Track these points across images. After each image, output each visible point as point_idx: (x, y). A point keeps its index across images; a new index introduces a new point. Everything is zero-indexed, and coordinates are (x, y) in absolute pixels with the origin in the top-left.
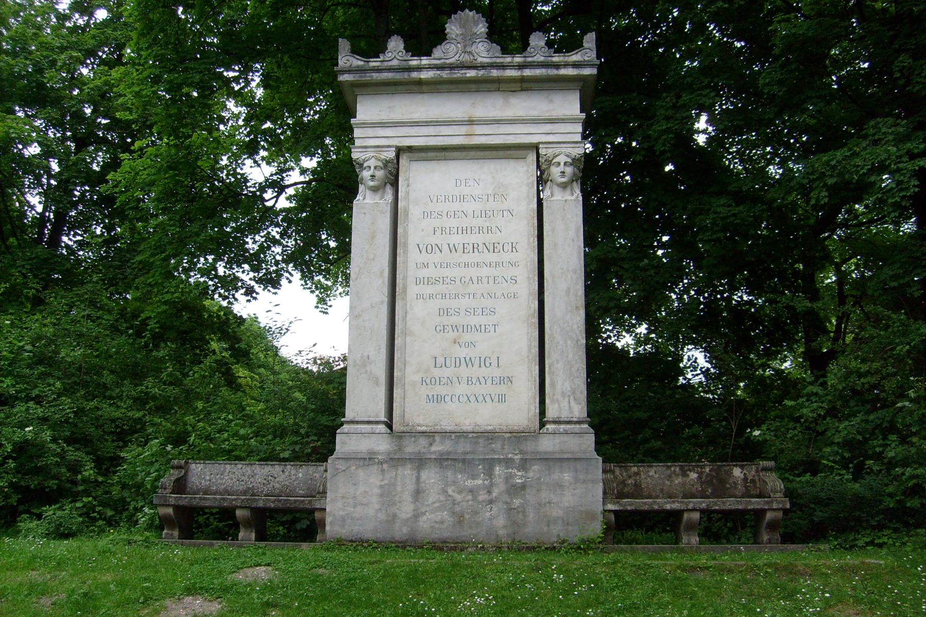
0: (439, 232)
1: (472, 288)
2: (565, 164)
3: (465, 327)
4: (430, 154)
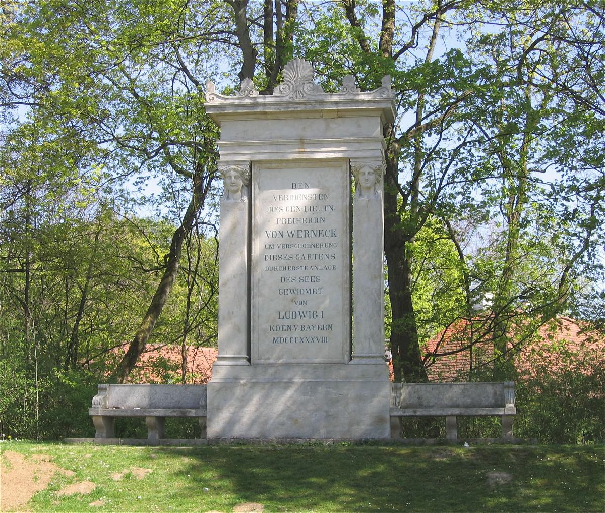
1: (304, 263)
2: (369, 173)
3: (300, 290)
4: (274, 165)
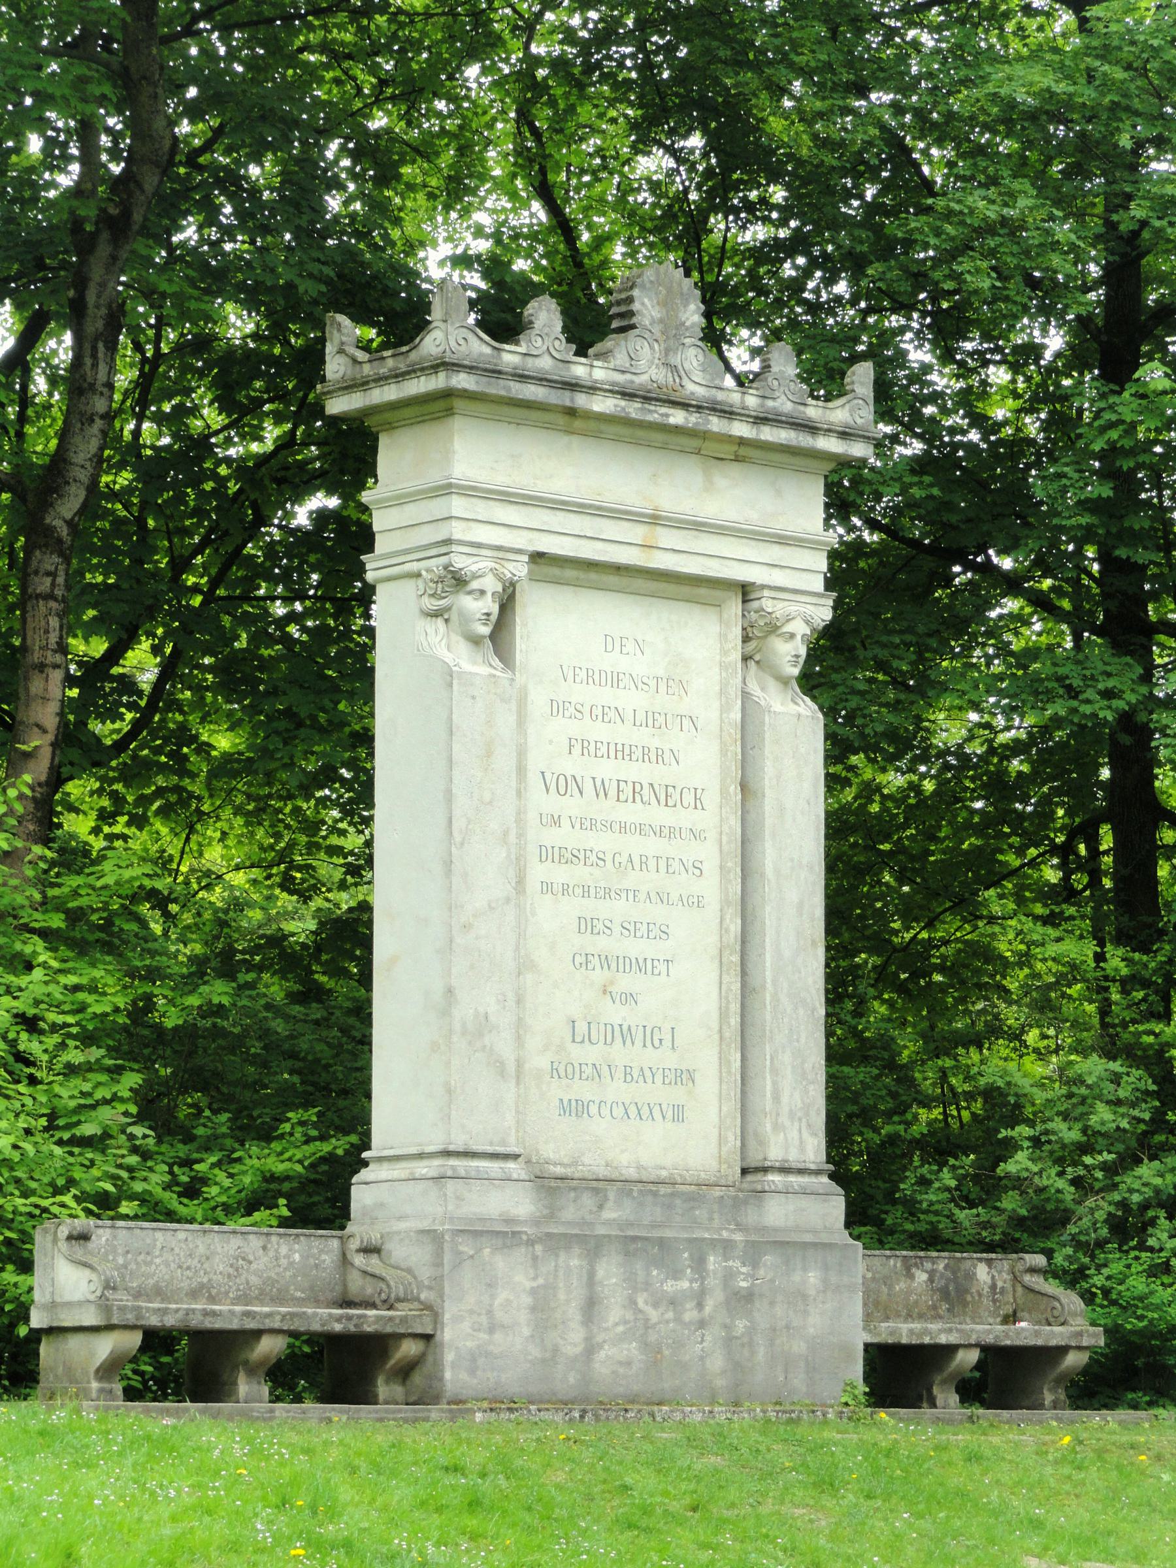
0: (577, 750)
1: (633, 879)
4: (570, 573)
